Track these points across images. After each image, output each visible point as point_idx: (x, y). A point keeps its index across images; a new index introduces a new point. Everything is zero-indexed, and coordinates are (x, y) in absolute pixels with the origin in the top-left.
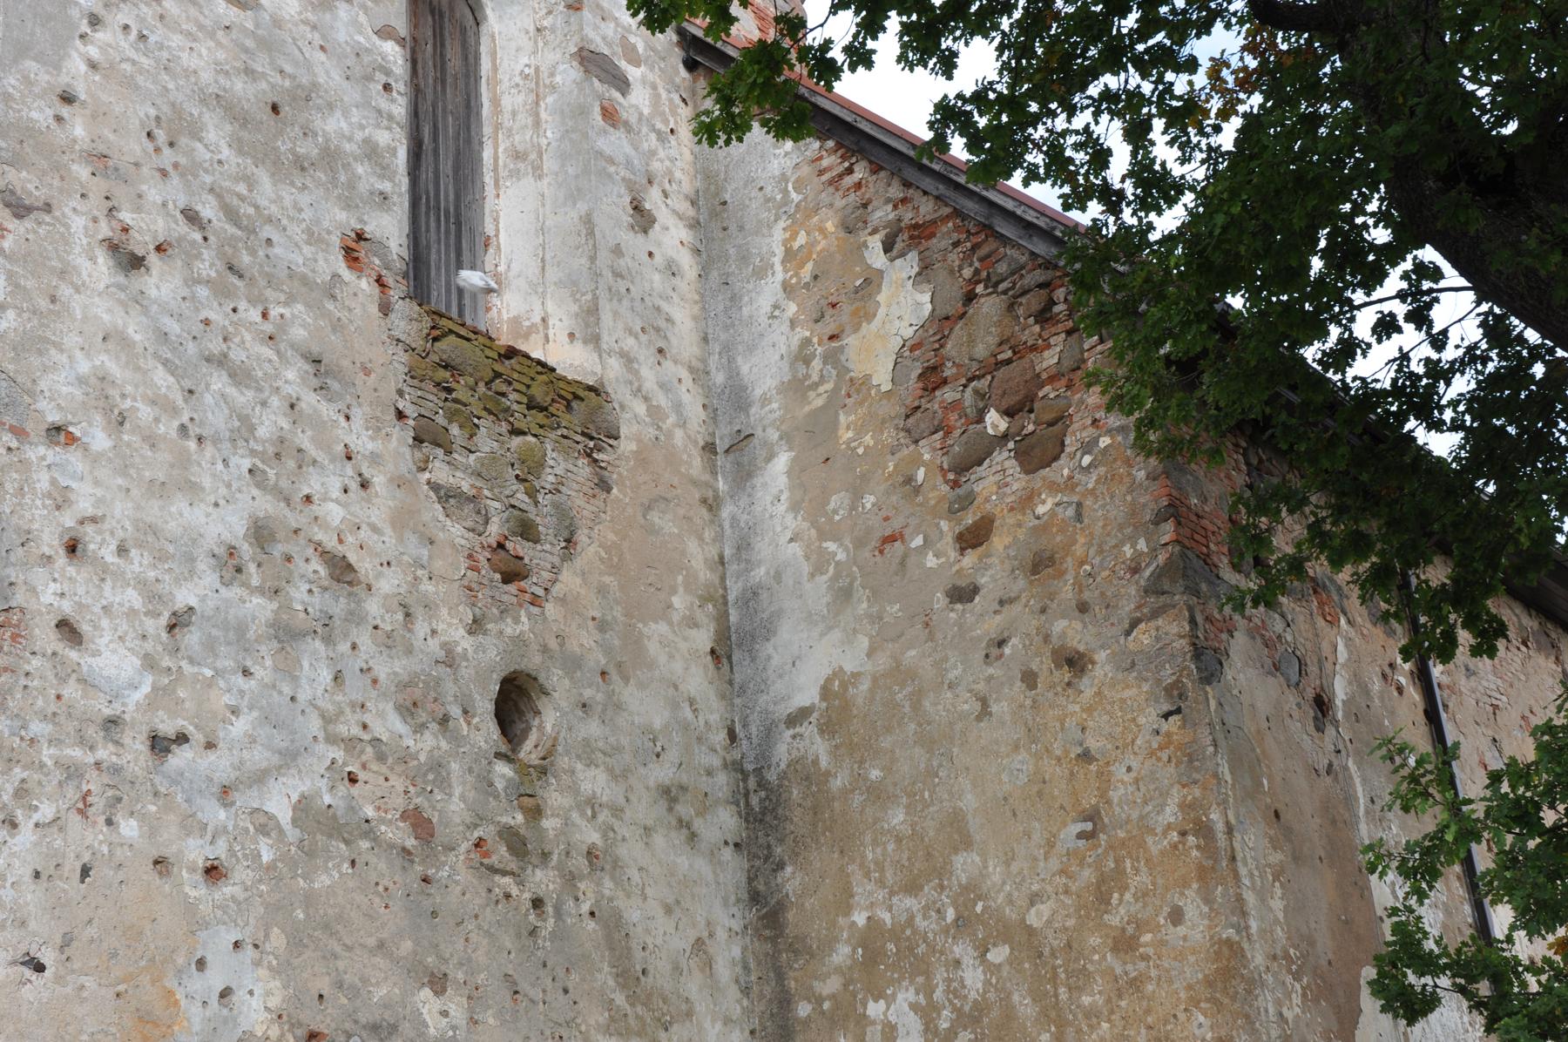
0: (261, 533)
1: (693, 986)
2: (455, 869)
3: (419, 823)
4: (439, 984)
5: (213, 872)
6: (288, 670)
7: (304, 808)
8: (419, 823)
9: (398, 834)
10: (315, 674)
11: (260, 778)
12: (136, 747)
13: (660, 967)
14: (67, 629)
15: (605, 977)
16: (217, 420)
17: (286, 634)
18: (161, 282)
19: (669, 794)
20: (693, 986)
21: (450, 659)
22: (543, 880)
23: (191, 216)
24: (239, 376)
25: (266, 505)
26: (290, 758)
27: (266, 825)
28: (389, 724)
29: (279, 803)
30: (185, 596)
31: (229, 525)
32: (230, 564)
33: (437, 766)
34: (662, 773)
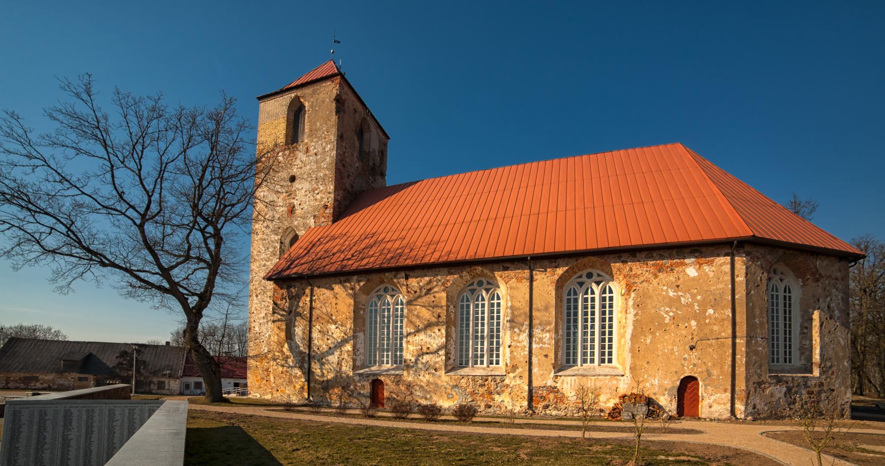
0: (266, 314)
6: (268, 325)
11: (266, 334)
16: (263, 306)
17: (267, 322)
18: (259, 297)
23: (261, 289)
24: (263, 301)
25: (266, 312)
27: (266, 337)
30: (261, 322)
31: (263, 315)
32: (264, 318)
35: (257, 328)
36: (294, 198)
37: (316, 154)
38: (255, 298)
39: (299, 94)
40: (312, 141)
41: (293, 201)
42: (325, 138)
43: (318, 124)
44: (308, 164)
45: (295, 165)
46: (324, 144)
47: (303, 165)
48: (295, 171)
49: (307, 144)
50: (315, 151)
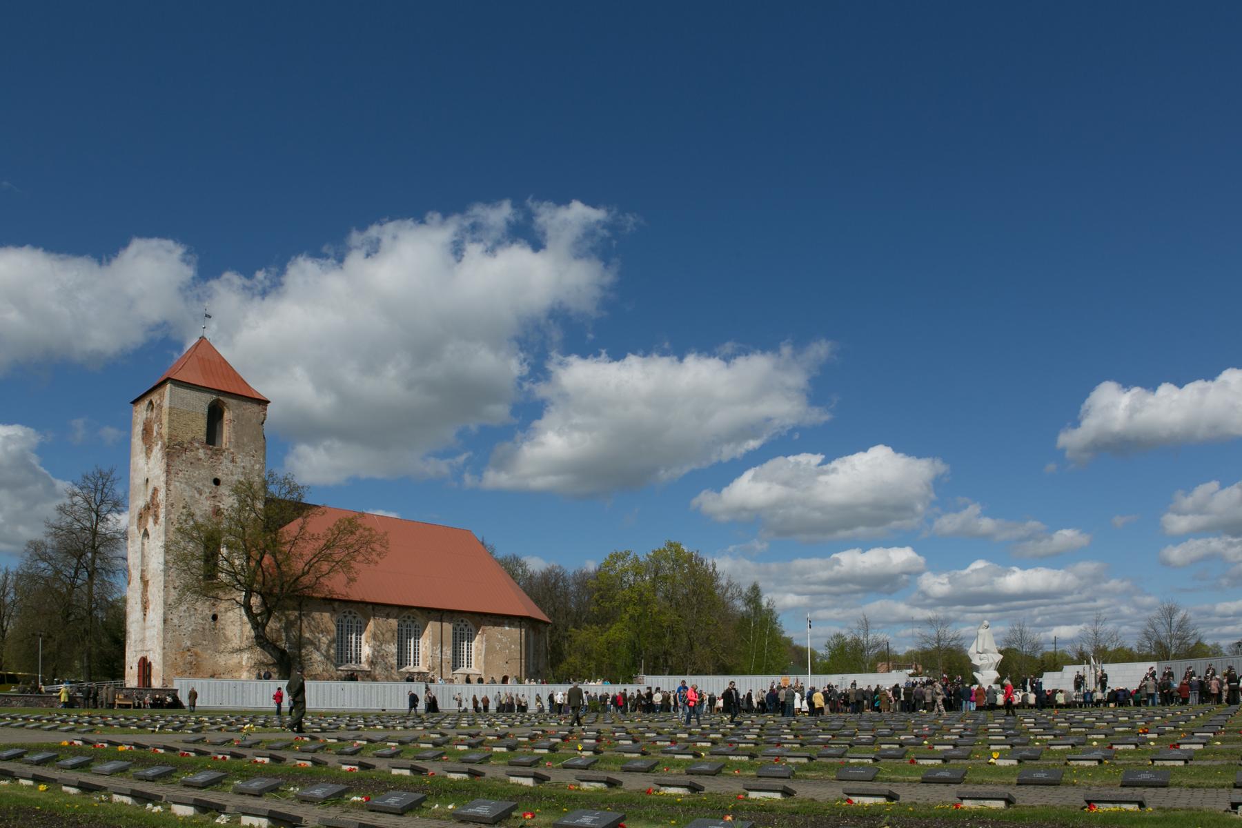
0: (188, 608)
1: (234, 638)
2: (207, 632)
3: (203, 628)
4: (205, 640)
5: (184, 635)
7: (192, 629)
8: (203, 628)
9: (201, 629)
10: (193, 618)
12: (177, 627)
13: (230, 637)
14: (171, 619)
15: (223, 638)
17: (190, 616)
19: (232, 622)
20: (234, 638)
21: (207, 614)
22: (217, 631)
26: (191, 626)
27: (189, 631)
28: (200, 621)
29: (190, 629)
32: (185, 611)
33: (205, 624)
34: (231, 620)
35: (176, 621)
36: (219, 502)
37: (244, 468)
38: (172, 590)
39: (221, 398)
40: (239, 453)
41: (219, 504)
42: (253, 456)
43: (245, 439)
44: (236, 474)
45: (219, 469)
46: (253, 462)
47: (229, 473)
48: (219, 475)
49: (232, 453)
50: (242, 464)
